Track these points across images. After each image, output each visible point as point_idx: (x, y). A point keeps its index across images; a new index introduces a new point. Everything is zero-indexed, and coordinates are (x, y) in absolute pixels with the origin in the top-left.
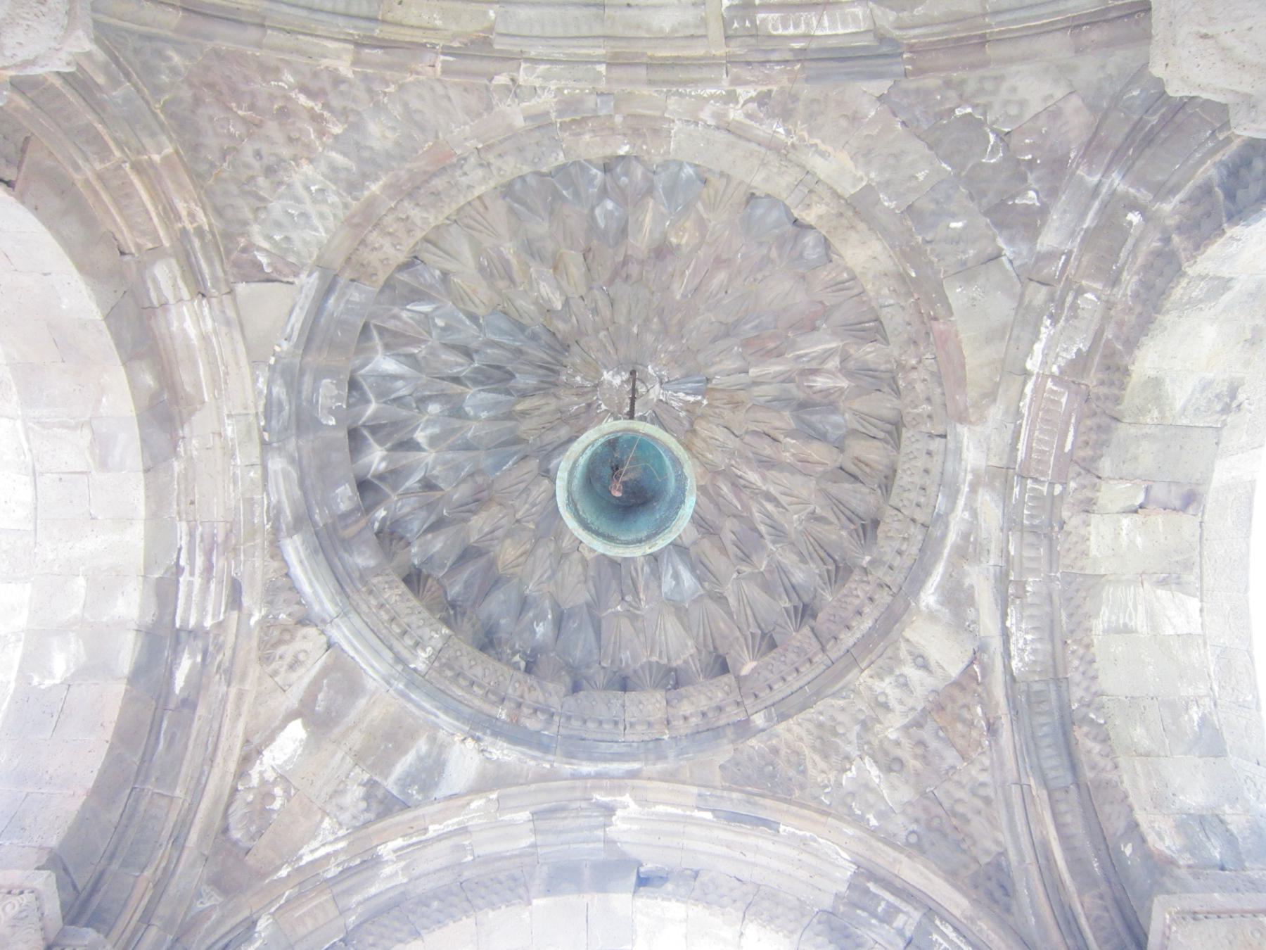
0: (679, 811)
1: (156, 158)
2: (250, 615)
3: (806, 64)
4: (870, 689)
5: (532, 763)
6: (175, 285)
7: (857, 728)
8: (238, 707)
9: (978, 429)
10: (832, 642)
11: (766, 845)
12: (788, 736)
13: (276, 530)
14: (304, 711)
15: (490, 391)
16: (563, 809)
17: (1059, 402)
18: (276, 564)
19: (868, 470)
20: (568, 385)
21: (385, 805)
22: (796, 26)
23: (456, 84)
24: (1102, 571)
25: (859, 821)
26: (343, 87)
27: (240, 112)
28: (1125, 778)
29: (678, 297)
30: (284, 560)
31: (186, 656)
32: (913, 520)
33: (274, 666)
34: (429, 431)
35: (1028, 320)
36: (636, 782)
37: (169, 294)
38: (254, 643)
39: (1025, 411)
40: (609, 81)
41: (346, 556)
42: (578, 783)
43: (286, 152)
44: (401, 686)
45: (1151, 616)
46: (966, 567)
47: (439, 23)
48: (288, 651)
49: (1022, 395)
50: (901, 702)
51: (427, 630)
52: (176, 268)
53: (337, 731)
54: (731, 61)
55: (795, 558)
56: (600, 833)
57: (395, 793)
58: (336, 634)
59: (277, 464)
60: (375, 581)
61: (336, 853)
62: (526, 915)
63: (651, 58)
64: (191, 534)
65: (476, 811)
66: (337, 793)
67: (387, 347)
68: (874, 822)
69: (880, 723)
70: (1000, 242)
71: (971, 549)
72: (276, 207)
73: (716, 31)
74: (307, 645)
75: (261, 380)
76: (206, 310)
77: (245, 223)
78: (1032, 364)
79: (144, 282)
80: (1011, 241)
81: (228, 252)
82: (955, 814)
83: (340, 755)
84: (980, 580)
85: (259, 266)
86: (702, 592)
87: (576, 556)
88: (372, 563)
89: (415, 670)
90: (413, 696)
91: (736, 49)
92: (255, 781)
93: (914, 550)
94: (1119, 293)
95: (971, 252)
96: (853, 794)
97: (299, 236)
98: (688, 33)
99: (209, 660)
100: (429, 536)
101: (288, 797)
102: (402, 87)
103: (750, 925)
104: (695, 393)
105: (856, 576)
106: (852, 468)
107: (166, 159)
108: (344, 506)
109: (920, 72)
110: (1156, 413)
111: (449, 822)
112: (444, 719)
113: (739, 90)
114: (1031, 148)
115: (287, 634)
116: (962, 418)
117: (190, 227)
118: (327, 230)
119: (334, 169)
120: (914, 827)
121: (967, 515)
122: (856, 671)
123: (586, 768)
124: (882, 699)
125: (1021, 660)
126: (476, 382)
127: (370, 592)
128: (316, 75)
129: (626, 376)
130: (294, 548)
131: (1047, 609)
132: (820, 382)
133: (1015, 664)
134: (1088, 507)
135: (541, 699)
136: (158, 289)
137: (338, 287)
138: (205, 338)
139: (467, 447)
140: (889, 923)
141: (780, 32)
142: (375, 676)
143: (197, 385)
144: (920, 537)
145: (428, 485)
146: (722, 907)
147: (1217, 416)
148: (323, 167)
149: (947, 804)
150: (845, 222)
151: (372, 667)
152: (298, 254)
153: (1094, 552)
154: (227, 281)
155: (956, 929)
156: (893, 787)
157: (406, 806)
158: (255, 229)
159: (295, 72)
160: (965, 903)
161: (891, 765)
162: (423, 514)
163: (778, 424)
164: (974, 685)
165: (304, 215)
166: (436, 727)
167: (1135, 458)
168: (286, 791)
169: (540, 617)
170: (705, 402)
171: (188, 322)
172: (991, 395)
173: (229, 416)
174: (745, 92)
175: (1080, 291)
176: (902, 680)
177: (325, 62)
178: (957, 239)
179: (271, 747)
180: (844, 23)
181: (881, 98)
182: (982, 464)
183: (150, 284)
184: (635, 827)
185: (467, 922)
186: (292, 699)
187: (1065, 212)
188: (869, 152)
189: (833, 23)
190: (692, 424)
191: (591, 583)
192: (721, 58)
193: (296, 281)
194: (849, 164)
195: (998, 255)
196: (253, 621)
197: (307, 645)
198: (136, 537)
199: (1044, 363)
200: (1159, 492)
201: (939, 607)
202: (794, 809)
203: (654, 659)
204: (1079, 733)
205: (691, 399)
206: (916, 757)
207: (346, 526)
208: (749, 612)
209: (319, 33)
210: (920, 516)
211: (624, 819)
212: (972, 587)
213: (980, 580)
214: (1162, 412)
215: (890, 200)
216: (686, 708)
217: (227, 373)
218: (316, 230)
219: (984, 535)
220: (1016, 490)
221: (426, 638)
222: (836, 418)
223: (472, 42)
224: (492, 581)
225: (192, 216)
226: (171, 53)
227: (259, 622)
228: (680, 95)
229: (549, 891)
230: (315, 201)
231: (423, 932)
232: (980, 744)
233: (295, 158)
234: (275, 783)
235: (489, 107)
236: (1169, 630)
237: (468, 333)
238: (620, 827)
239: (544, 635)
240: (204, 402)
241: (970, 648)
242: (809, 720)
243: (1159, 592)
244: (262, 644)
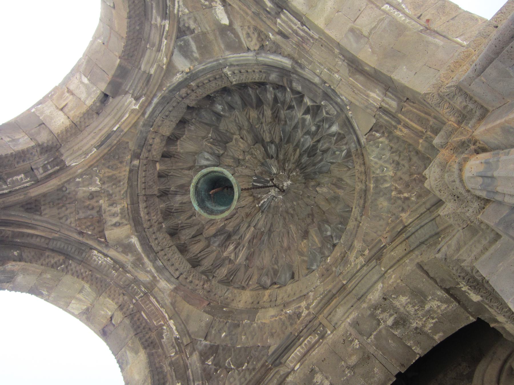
0: (122, 121)
1: (421, 141)
2: (273, 35)
3: (295, 337)
4: (120, 204)
5: (168, 85)
6: (387, 104)
7: (111, 192)
8: (243, 10)
9: (168, 292)
10: (145, 199)
11: (93, 142)
12: (123, 169)
13: (297, 62)
14: (230, 27)
15: (308, 148)
16: (147, 85)
17: (155, 321)
18: (286, 53)
19: (193, 243)
20: (295, 169)
21: (182, 32)
22: (305, 344)
23: (376, 239)
24: (101, 297)
25: (81, 175)
26: (400, 209)
27: (416, 176)
28: (37, 266)
29: (291, 226)
30: (286, 57)
31: (272, 6)
32: (162, 250)
33: (252, 29)
35: (184, 331)
36: (140, 114)
37: (387, 99)
38: (263, 29)
39: (162, 309)
40: (340, 281)
42: (152, 95)
43: (399, 174)
44: (221, 61)
45: (80, 300)
46: (134, 258)
47: (393, 253)
48: (255, 36)
49: (166, 312)
50: (109, 210)
51: (238, 79)
52: (390, 109)
53: (218, 33)
54: (315, 318)
55: (185, 201)
56: (131, 92)
57: (185, 37)
60: (264, 75)
61: (174, 8)
62: (117, 54)
63: (336, 297)
64: (312, 37)
65: (163, 58)
66: (195, 20)
67: (339, 134)
68: (78, 180)
69: (108, 200)
70: (207, 343)
71: (138, 263)
72: (388, 154)
73: (325, 322)
74: (253, 43)
75: (345, 99)
76: (376, 104)
78: (171, 322)
79: (396, 96)
80: (206, 346)
81: (386, 128)
82: (63, 206)
83: (208, 29)
84: (127, 259)
85: (377, 131)
86: (196, 165)
87: (237, 133)
89: (225, 67)
90: (215, 63)
91: (316, 322)
93: (153, 244)
94: (167, 363)
95: (213, 332)
96: (91, 178)
97: (377, 151)
98: (332, 314)
99: (265, 12)
101: (203, 5)
102: (388, 224)
103: (69, 123)
104: (262, 205)
105: (161, 220)
106: (198, 238)
109: (263, 366)
111: (164, 48)
112: (201, 67)
113: (307, 312)
114: (220, 375)
116: (176, 289)
117: (399, 126)
118: (372, 160)
119: (385, 181)
120: (68, 192)
121: (148, 269)
122: (129, 202)
123: (155, 100)
124: (115, 205)
125: (95, 255)
126: (314, 146)
129: (285, 188)
130: (287, 63)
131: (104, 273)
132: (231, 247)
133: (95, 252)
134: (121, 307)
135: (191, 98)
136: (391, 98)
137: (357, 144)
138: (368, 96)
139: (296, 127)
140: (42, 167)
141: (308, 339)
142: (229, 56)
143: (356, 80)
144: (155, 249)
146: (81, 118)
148: (387, 178)
149: (68, 206)
150: (255, 303)
152: (372, 146)
153: (107, 299)
155: (27, 187)
156: (85, 192)
157: (177, 38)
158: (387, 142)
160: (33, 195)
161: (92, 196)
162: (282, 99)
163: (231, 224)
164: (98, 236)
165: (380, 159)
166: (200, 63)
168: (205, 5)
169: (223, 110)
170: (257, 206)
171: (375, 96)
172: (173, 304)
173: (341, 80)
174: (305, 313)
175: (176, 353)
176: (116, 215)
177: (408, 213)
178: (220, 332)
179: (223, 10)
180: (293, 358)
181: (269, 347)
182: (158, 285)
183: (393, 97)
184: (126, 104)
185: (125, 35)
186: (237, 26)
187: (197, 369)
188: (261, 330)
189: (296, 354)
190: (254, 197)
191: (225, 132)
192: (319, 316)
193: (365, 137)
194: (264, 321)
195: (205, 339)
197: (253, 43)
198: (320, 23)
199: (169, 326)
200: (111, 328)
201: (129, 241)
202: (98, 158)
203: (184, 136)
204: (62, 258)
205: (262, 202)
206: (89, 205)
207: (287, 80)
208: (178, 175)
209: (416, 221)
210: (162, 253)
211: (131, 102)
212: (127, 255)
213: (127, 259)
215: (246, 323)
216: (157, 140)
217: (354, 92)
218: (374, 157)
219: (139, 270)
220: (143, 289)
221: (235, 77)
222: (216, 244)
223: (382, 255)
224: (245, 104)
225: (401, 131)
228: (321, 295)
229: (120, 66)
230: (381, 166)
231: (129, 20)
232: (79, 226)
233: (395, 174)
234: (210, 4)
236: (73, 301)
237: (328, 157)
238: (129, 99)
239: (217, 108)
240: (350, 77)
241: (111, 242)
242: (124, 179)
243: (86, 307)
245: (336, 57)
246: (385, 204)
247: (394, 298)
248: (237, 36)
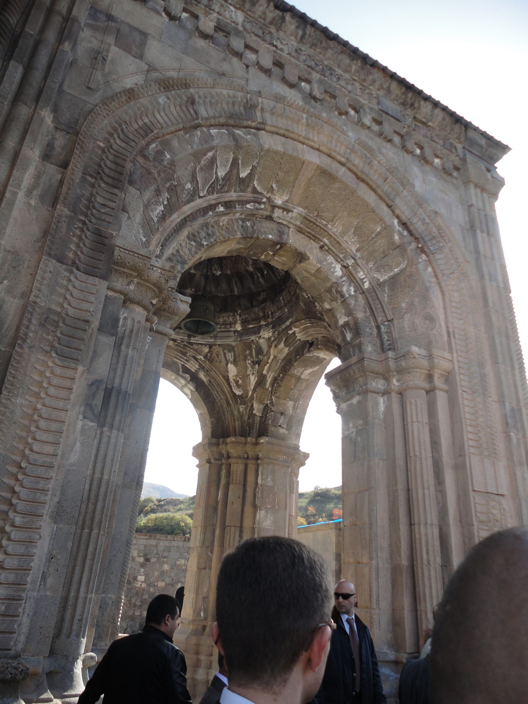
48: (214, 355)
58: (218, 343)
100: (219, 288)
123: (284, 326)
166: (253, 341)
186: (224, 362)
197: (216, 350)
236: (313, 272)
244: (209, 360)
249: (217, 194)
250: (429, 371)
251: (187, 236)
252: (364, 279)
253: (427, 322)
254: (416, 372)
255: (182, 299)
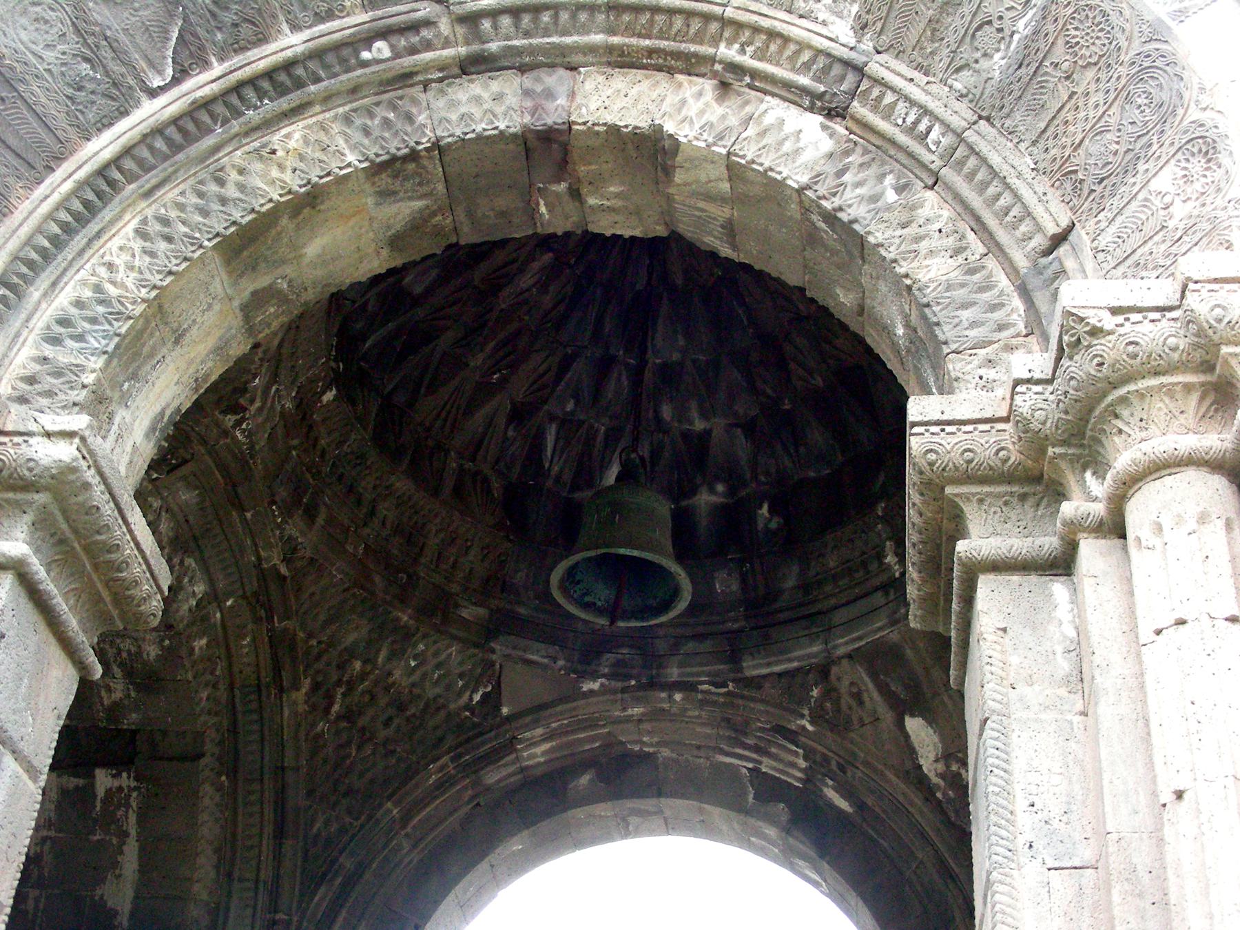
1: (395, 812)
2: (804, 727)
6: (504, 766)
14: (902, 709)
26: (320, 679)
30: (765, 677)
33: (855, 719)
34: (694, 414)
37: (511, 769)
41: (778, 605)
43: (383, 701)
45: (709, 197)
48: (846, 700)
58: (841, 651)
59: (674, 673)
64: (728, 754)
72: (431, 692)
76: (528, 734)
77: (449, 715)
85: (486, 696)
88: (795, 569)
92: (942, 783)
100: (802, 450)
102: (310, 635)
107: (396, 804)
108: (735, 587)
110: (439, 218)
115: (830, 693)
127: (819, 584)
128: (314, 707)
130: (753, 667)
136: (510, 775)
143: (592, 739)
145: (749, 428)
147: (425, 162)
151: (881, 629)
154: (499, 727)
158: (452, 706)
159: (313, 725)
167: (502, 214)
171: (537, 751)
186: (887, 716)
196: (810, 728)
214: (434, 214)
226: (315, 830)
227: (811, 723)
235: (312, 561)
236: (725, 186)
237: (581, 370)
245: (658, 744)
246: (351, 638)
247: (163, 640)
248: (883, 688)
249: (221, 60)
250: (1207, 366)
251: (137, 231)
252: (916, 123)
253: (1197, 165)
254: (1141, 395)
255: (50, 427)
